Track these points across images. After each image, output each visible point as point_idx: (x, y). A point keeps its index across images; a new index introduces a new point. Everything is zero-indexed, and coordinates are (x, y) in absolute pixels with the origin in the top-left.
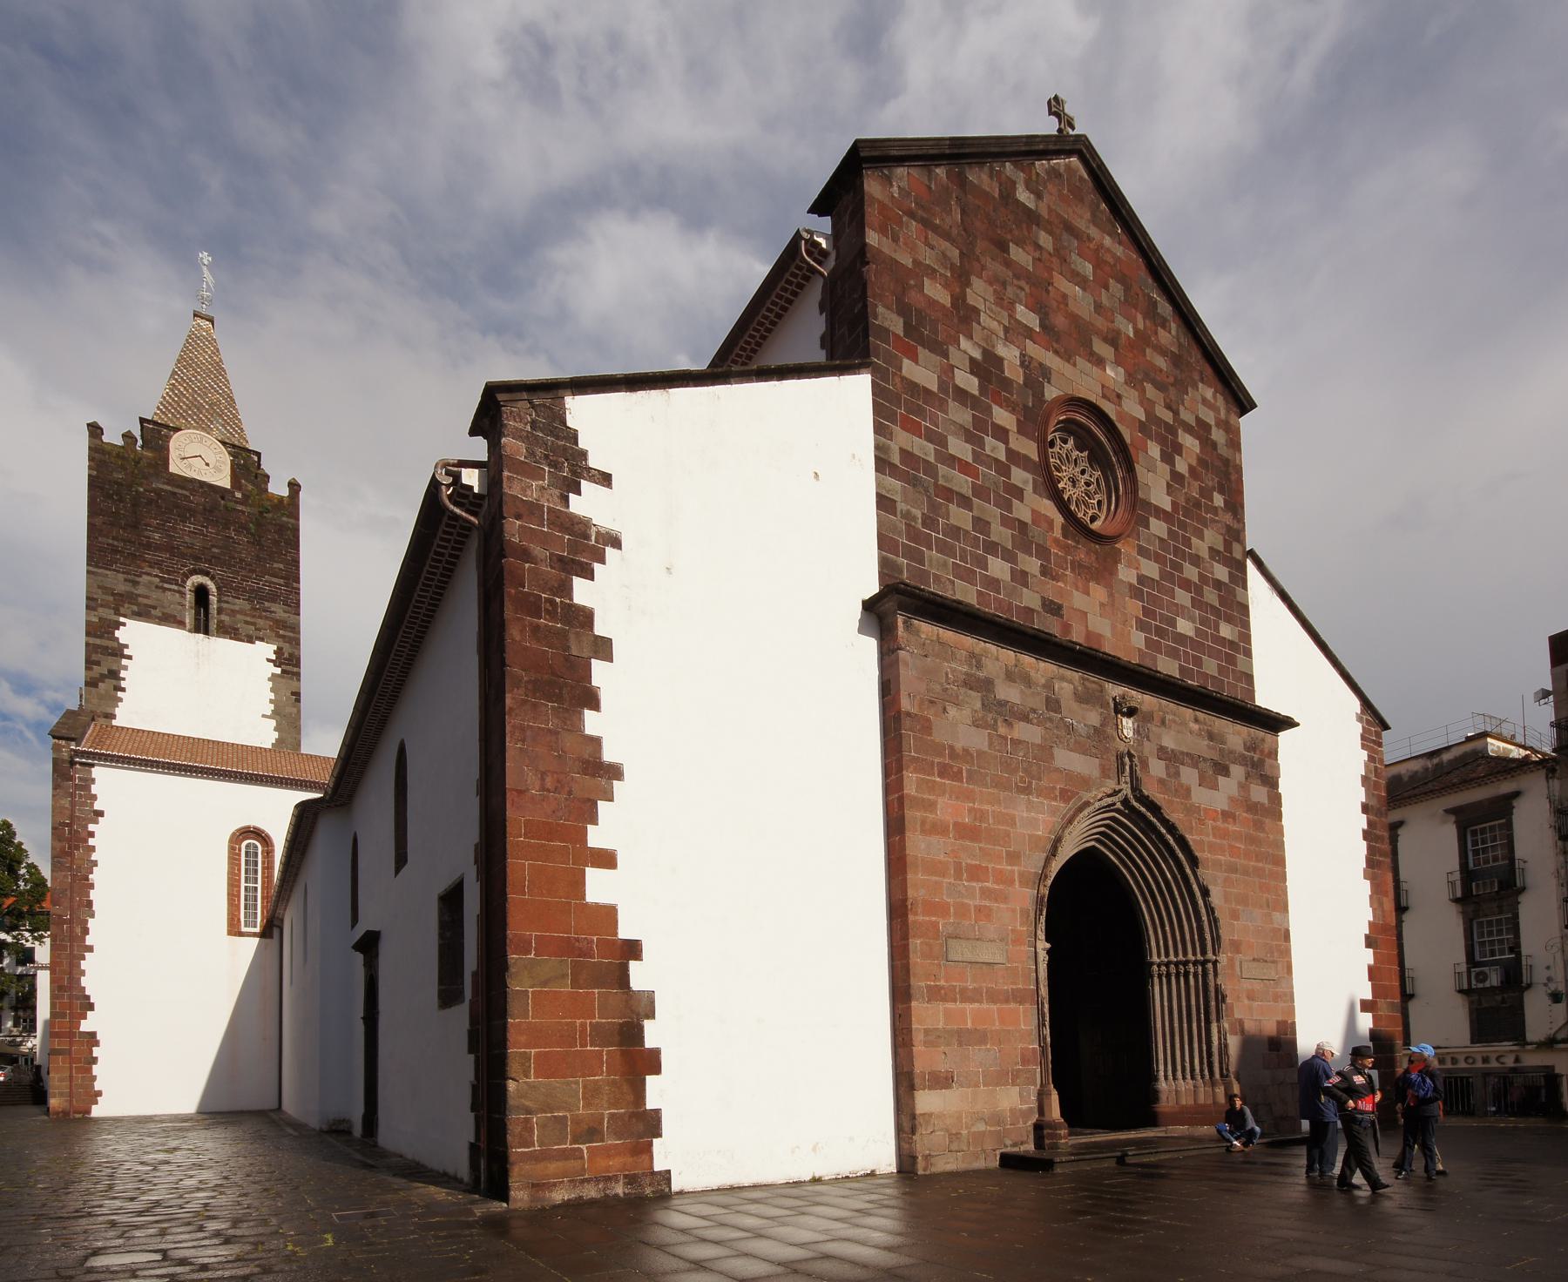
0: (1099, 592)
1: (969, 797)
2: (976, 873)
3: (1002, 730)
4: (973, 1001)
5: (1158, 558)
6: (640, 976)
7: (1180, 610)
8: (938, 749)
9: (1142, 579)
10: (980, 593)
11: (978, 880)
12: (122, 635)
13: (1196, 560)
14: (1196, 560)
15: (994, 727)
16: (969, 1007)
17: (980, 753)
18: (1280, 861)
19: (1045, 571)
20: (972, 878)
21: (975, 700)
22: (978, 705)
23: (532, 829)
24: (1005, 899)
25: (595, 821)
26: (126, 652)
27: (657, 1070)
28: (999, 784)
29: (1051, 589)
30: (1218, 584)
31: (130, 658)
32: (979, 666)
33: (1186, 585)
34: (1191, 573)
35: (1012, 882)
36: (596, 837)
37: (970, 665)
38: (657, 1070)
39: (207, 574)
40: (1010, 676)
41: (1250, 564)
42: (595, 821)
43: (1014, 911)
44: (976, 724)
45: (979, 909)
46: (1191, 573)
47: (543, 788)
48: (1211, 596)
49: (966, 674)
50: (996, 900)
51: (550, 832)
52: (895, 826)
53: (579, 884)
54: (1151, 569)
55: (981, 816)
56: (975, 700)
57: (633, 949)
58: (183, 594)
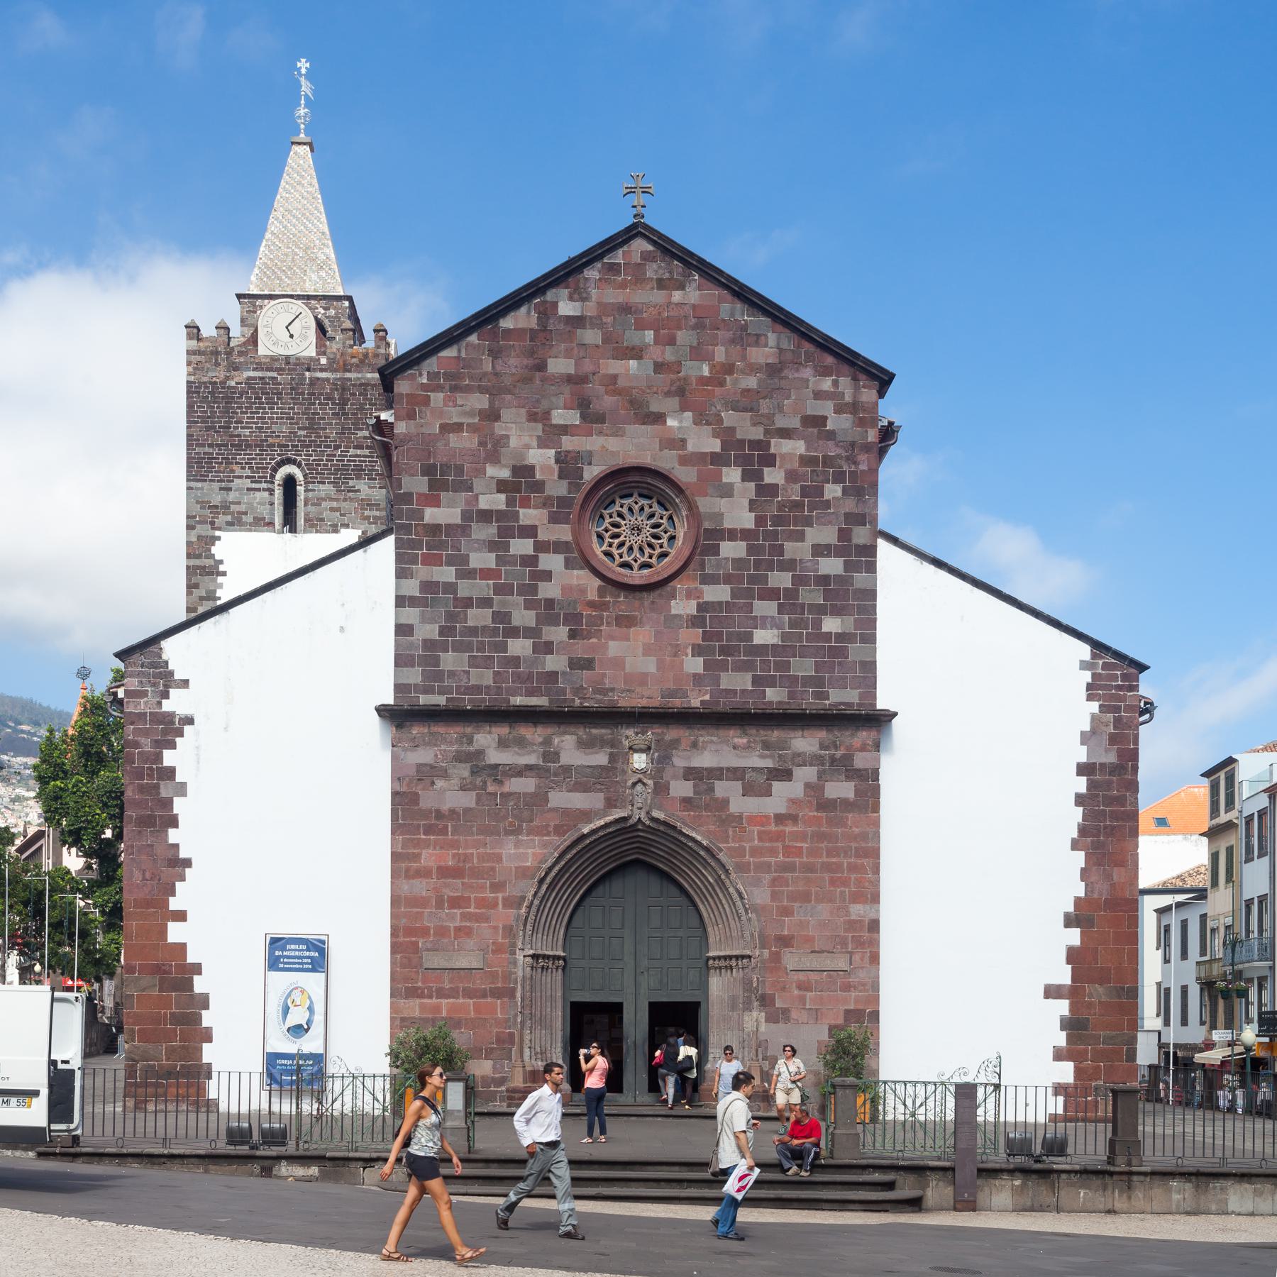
0: (643, 634)
1: (454, 845)
2: (455, 903)
3: (491, 788)
4: (448, 997)
5: (728, 579)
6: (200, 985)
7: (762, 622)
8: (426, 814)
9: (702, 607)
10: (496, 674)
11: (460, 907)
12: (218, 550)
13: (789, 565)
14: (789, 565)
15: (484, 787)
16: (444, 1001)
17: (467, 810)
18: (874, 854)
19: (573, 635)
20: (451, 907)
21: (464, 771)
22: (466, 774)
23: (137, 904)
24: (487, 920)
25: (173, 894)
26: (222, 568)
27: (210, 1040)
28: (485, 831)
29: (580, 649)
30: (824, 580)
31: (224, 574)
32: (470, 742)
33: (772, 594)
34: (781, 580)
35: (495, 905)
36: (174, 904)
37: (462, 743)
38: (209, 1039)
39: (294, 462)
40: (503, 744)
41: (882, 544)
42: (173, 894)
43: (495, 928)
44: (463, 788)
45: (458, 929)
46: (781, 580)
47: (144, 879)
48: (811, 596)
49: (457, 751)
50: (477, 921)
51: (148, 903)
52: (1117, 655)
53: (163, 932)
54: (718, 593)
55: (467, 858)
56: (464, 771)
57: (197, 969)
58: (271, 491)
